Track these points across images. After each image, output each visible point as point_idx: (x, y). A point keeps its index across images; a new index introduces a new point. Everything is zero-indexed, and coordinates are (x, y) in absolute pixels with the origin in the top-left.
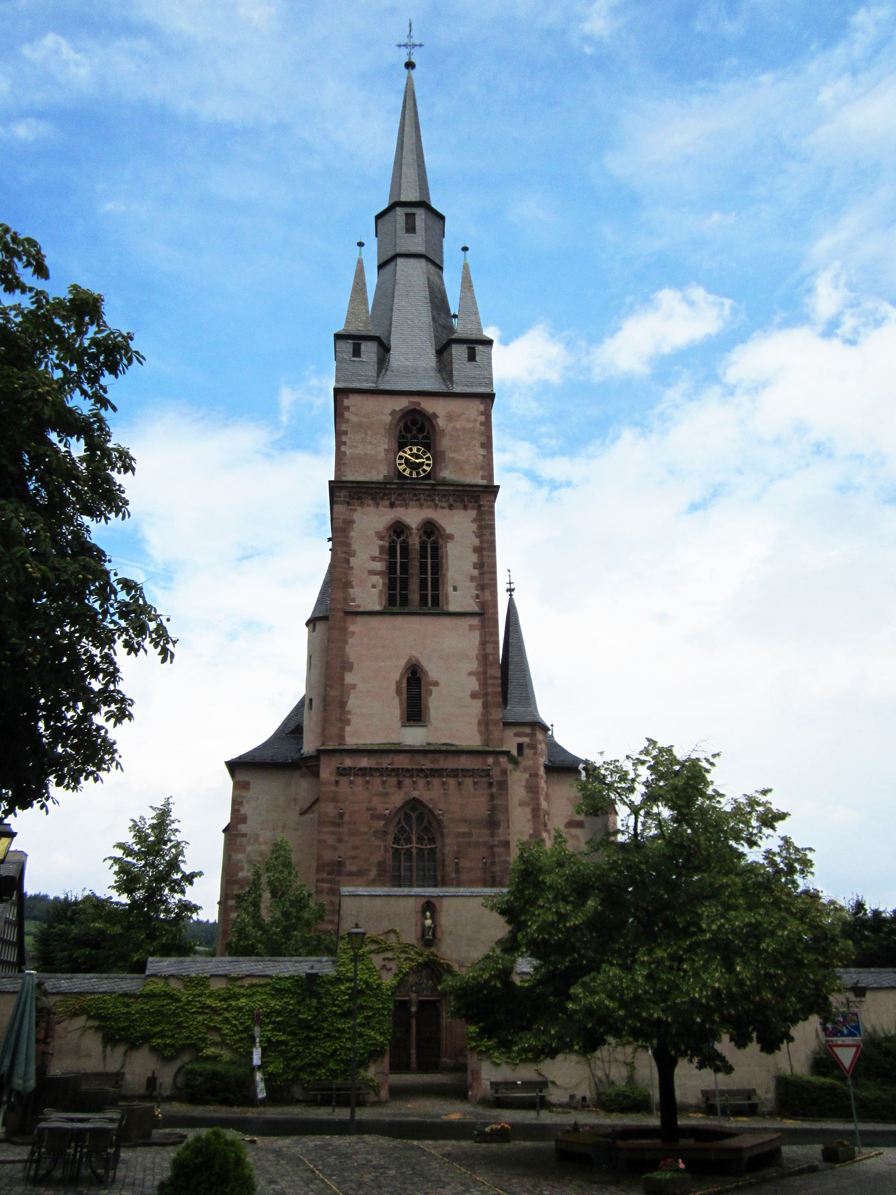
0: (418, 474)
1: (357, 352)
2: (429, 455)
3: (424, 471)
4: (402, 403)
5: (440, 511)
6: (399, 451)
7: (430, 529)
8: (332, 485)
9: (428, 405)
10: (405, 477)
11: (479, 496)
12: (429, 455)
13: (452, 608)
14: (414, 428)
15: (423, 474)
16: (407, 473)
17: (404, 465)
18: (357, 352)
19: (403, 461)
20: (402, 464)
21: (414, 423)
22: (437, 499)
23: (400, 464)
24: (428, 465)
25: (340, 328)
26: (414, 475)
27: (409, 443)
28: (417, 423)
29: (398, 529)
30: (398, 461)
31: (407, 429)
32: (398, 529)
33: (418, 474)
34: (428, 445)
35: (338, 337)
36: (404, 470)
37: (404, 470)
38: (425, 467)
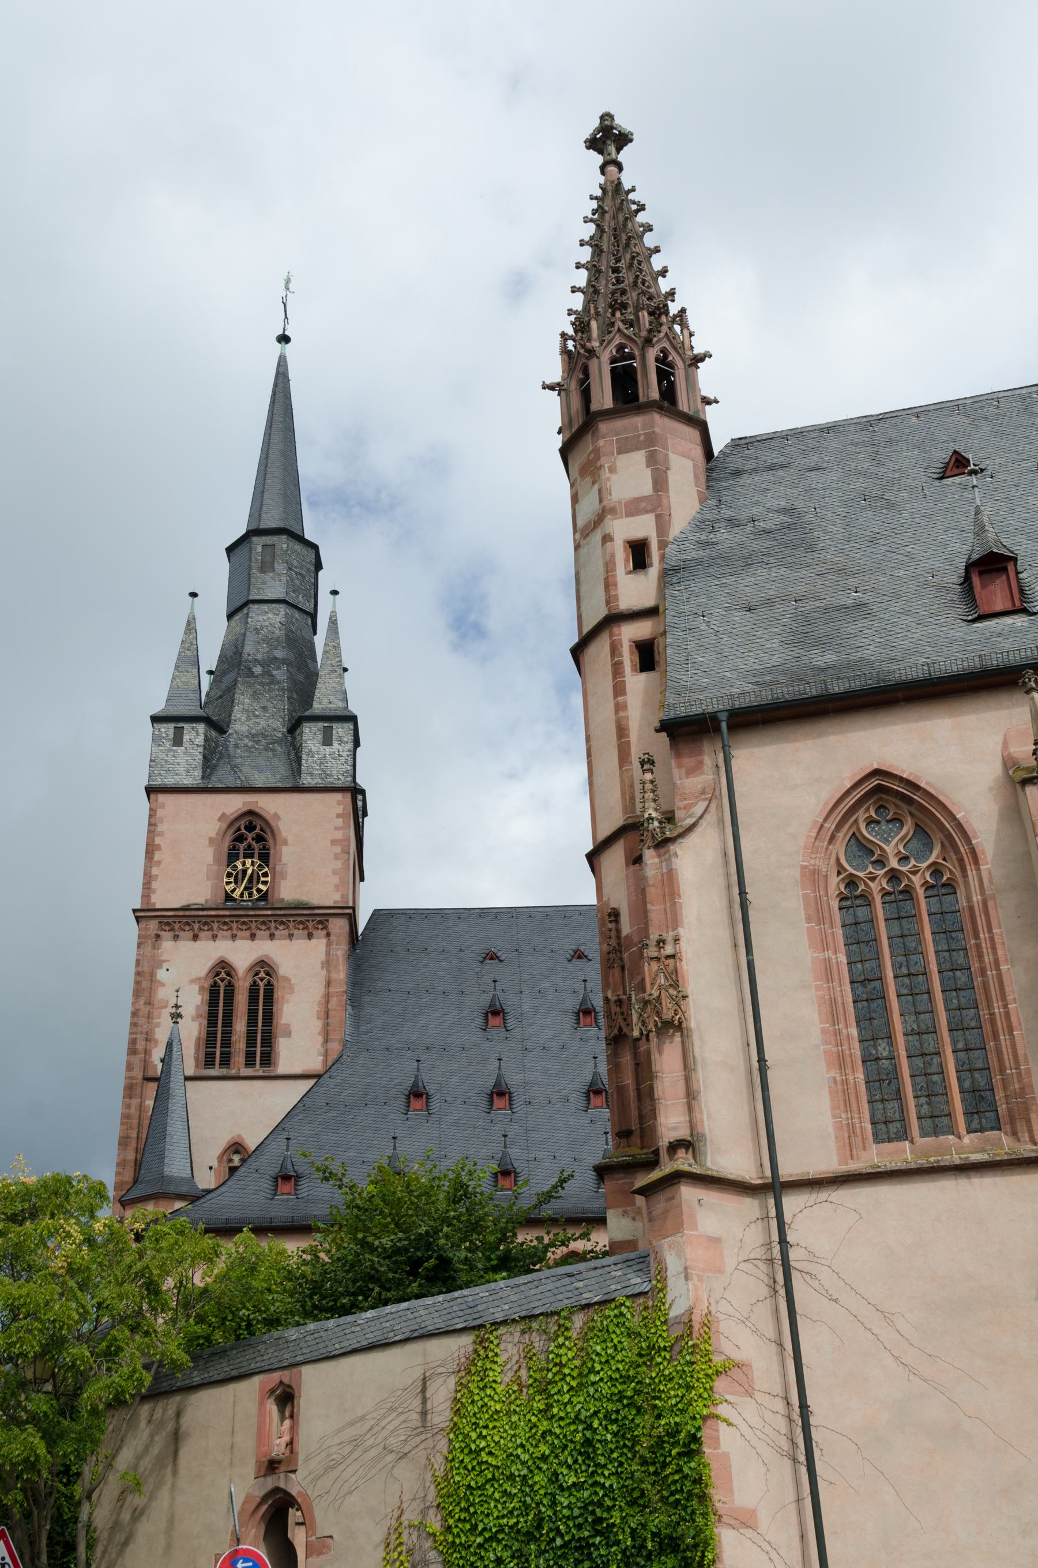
0: (250, 895)
1: (178, 741)
2: (266, 869)
3: (259, 891)
4: (235, 804)
5: (276, 943)
6: (228, 866)
7: (264, 968)
8: (139, 914)
9: (268, 805)
10: (234, 900)
11: (327, 921)
12: (266, 869)
13: (282, 1069)
14: (252, 835)
15: (256, 895)
16: (236, 895)
17: (233, 885)
18: (178, 741)
19: (232, 879)
20: (231, 882)
21: (250, 827)
22: (273, 925)
23: (228, 883)
24: (265, 883)
25: (159, 706)
26: (246, 895)
27: (241, 855)
28: (255, 827)
29: (223, 968)
30: (226, 880)
31: (240, 839)
32: (223, 968)
33: (250, 895)
34: (265, 858)
35: (155, 719)
36: (233, 891)
37: (233, 891)
38: (261, 886)
